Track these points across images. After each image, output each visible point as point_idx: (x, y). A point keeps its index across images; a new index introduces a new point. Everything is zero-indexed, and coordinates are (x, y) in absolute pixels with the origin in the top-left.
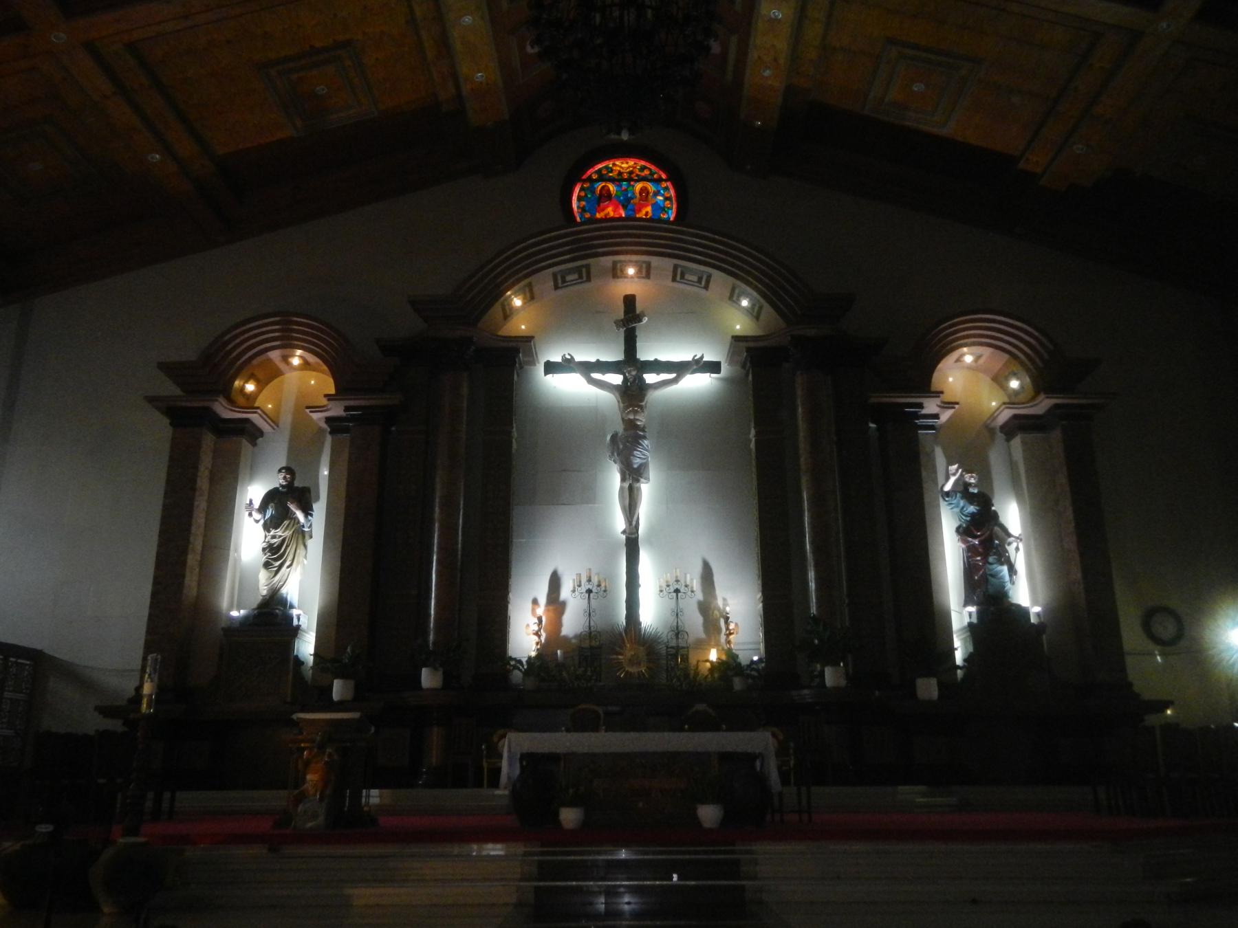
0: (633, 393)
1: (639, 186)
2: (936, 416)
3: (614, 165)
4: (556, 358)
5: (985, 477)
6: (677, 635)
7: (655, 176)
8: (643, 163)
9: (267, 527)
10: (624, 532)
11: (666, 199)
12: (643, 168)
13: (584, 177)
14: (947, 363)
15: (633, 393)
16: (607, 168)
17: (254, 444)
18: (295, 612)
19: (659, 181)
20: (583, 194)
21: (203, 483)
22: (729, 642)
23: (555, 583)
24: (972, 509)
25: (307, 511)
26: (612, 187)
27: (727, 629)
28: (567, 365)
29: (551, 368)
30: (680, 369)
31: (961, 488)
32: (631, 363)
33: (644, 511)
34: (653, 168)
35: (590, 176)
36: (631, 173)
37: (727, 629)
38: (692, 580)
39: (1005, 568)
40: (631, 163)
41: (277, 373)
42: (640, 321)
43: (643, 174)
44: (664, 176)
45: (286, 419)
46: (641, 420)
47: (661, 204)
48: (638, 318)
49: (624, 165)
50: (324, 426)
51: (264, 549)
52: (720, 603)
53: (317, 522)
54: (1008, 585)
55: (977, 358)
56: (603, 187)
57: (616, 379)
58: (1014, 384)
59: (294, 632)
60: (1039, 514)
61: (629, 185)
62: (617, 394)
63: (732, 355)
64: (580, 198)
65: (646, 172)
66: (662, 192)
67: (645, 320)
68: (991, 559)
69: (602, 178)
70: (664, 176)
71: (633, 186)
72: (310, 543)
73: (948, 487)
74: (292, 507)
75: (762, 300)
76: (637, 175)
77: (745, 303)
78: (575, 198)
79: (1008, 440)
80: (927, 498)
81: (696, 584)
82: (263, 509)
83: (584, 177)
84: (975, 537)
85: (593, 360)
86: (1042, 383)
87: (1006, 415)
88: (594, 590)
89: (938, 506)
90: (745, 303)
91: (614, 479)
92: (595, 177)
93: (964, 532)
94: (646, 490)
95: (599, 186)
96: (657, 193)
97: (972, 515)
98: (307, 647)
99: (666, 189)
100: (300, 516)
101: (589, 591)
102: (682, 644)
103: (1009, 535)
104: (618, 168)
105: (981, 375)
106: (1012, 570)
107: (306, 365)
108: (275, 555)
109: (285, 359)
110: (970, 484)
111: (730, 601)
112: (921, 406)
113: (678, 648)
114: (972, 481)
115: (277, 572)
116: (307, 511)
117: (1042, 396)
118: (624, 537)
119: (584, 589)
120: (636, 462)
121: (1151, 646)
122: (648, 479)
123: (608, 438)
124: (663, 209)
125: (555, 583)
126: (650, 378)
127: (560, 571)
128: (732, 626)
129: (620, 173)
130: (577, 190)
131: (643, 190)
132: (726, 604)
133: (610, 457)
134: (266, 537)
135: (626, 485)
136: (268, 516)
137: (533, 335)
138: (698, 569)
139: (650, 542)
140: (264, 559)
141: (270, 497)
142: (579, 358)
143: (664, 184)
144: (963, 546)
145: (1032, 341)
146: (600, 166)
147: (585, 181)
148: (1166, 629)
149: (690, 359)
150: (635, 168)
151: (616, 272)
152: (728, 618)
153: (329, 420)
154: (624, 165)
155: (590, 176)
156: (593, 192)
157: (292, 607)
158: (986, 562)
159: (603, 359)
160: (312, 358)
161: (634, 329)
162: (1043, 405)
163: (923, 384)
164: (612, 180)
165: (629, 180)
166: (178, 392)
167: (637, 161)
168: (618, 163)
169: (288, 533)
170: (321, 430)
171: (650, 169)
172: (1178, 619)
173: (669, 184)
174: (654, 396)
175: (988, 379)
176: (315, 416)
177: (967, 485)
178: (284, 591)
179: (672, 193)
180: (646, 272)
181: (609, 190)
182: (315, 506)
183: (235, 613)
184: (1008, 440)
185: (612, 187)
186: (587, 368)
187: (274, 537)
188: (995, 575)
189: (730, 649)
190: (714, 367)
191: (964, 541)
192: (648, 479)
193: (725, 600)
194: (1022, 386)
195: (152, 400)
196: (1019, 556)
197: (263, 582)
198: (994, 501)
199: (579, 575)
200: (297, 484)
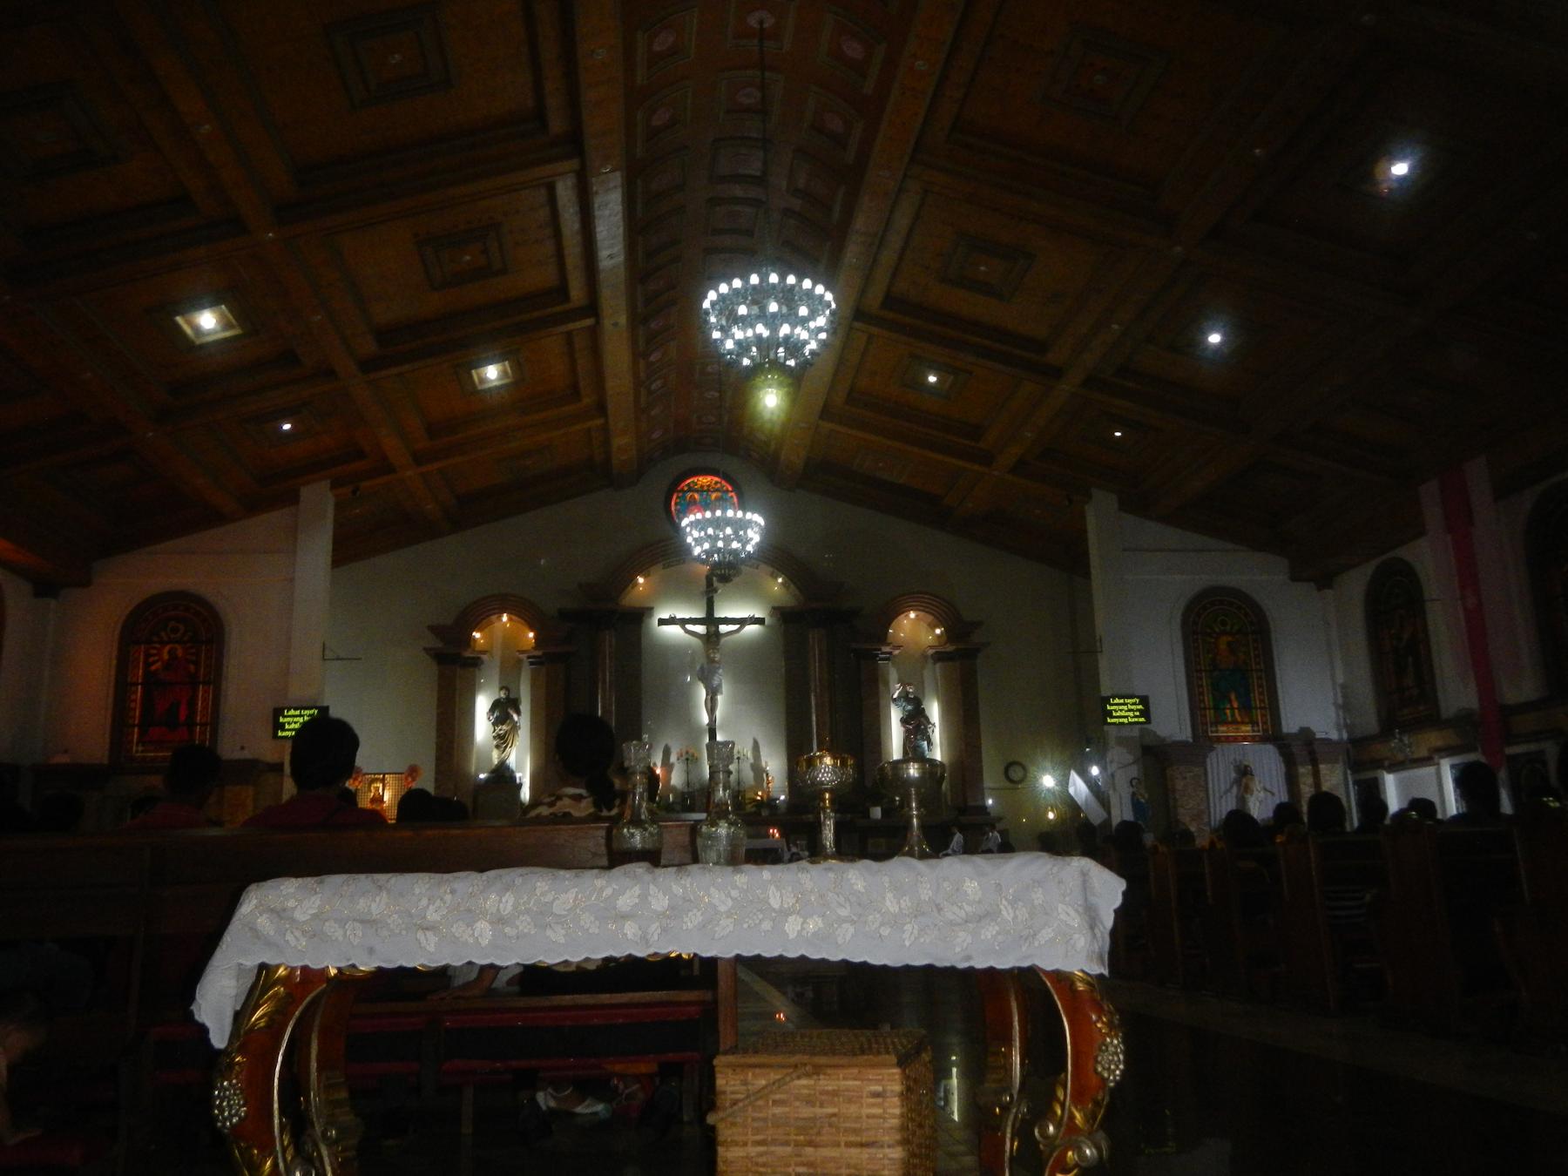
0: (712, 638)
2: (890, 653)
4: (665, 616)
5: (921, 686)
6: (739, 783)
8: (716, 479)
9: (493, 724)
10: (708, 725)
12: (716, 483)
14: (903, 616)
15: (712, 638)
16: (693, 482)
17: (479, 669)
18: (518, 775)
21: (457, 699)
22: (769, 788)
23: (667, 753)
24: (909, 707)
25: (519, 713)
26: (696, 496)
27: (768, 780)
28: (672, 621)
29: (662, 622)
30: (742, 622)
31: (903, 695)
32: (710, 620)
33: (718, 713)
34: (724, 483)
35: (682, 489)
36: (709, 486)
37: (768, 780)
38: (747, 752)
39: (926, 743)
40: (709, 479)
41: (492, 623)
42: (716, 592)
45: (497, 653)
46: (718, 657)
48: (715, 591)
50: (525, 659)
51: (494, 737)
52: (763, 764)
53: (523, 720)
54: (927, 752)
55: (917, 616)
57: (700, 629)
58: (938, 631)
59: (520, 785)
60: (946, 712)
61: (707, 495)
62: (702, 641)
63: (771, 616)
64: (676, 504)
65: (719, 485)
67: (720, 591)
68: (919, 737)
69: (690, 490)
70: (730, 489)
72: (519, 732)
73: (895, 696)
74: (511, 712)
75: (789, 582)
77: (780, 580)
78: (673, 503)
79: (935, 663)
80: (882, 702)
81: (750, 755)
82: (492, 710)
83: (679, 488)
84: (911, 724)
85: (687, 617)
86: (952, 634)
87: (931, 652)
88: (690, 758)
89: (890, 704)
90: (780, 580)
91: (702, 693)
92: (686, 489)
93: (904, 721)
94: (719, 698)
95: (689, 494)
97: (909, 711)
98: (526, 794)
100: (515, 717)
101: (687, 759)
102: (742, 789)
103: (930, 723)
105: (922, 623)
106: (930, 743)
107: (510, 620)
108: (502, 741)
109: (500, 618)
110: (909, 692)
111: (769, 764)
112: (880, 650)
113: (739, 792)
114: (911, 690)
115: (504, 751)
116: (519, 713)
117: (948, 645)
118: (707, 727)
119: (684, 757)
120: (716, 683)
121: (1011, 785)
122: (722, 693)
123: (698, 667)
125: (667, 753)
126: (723, 628)
127: (670, 744)
128: (770, 778)
129: (702, 486)
130: (675, 497)
132: (767, 765)
133: (700, 679)
134: (495, 730)
135: (709, 697)
136: (495, 715)
137: (651, 605)
138: (750, 744)
139: (722, 727)
140: (495, 742)
141: (496, 706)
142: (679, 616)
143: (730, 494)
144: (902, 729)
145: (945, 609)
146: (689, 481)
147: (680, 491)
148: (1016, 773)
149: (747, 616)
152: (767, 774)
153: (529, 657)
154: (704, 480)
155: (682, 489)
157: (513, 772)
158: (915, 738)
159: (693, 617)
160: (514, 617)
161: (712, 597)
162: (950, 648)
163: (882, 638)
164: (697, 491)
165: (709, 490)
166: (440, 645)
167: (713, 477)
168: (700, 479)
169: (509, 727)
170: (520, 661)
172: (1024, 768)
173: (733, 494)
174: (723, 640)
175: (925, 625)
176: (521, 656)
177: (908, 693)
178: (508, 762)
181: (695, 498)
182: (521, 707)
183: (482, 776)
184: (935, 663)
185: (696, 496)
186: (683, 622)
187: (500, 730)
188: (920, 746)
189: (769, 792)
190: (760, 621)
191: (904, 727)
192: (722, 693)
193: (766, 763)
194: (941, 632)
196: (937, 735)
197: (495, 757)
198: (924, 703)
199: (681, 750)
200: (512, 696)
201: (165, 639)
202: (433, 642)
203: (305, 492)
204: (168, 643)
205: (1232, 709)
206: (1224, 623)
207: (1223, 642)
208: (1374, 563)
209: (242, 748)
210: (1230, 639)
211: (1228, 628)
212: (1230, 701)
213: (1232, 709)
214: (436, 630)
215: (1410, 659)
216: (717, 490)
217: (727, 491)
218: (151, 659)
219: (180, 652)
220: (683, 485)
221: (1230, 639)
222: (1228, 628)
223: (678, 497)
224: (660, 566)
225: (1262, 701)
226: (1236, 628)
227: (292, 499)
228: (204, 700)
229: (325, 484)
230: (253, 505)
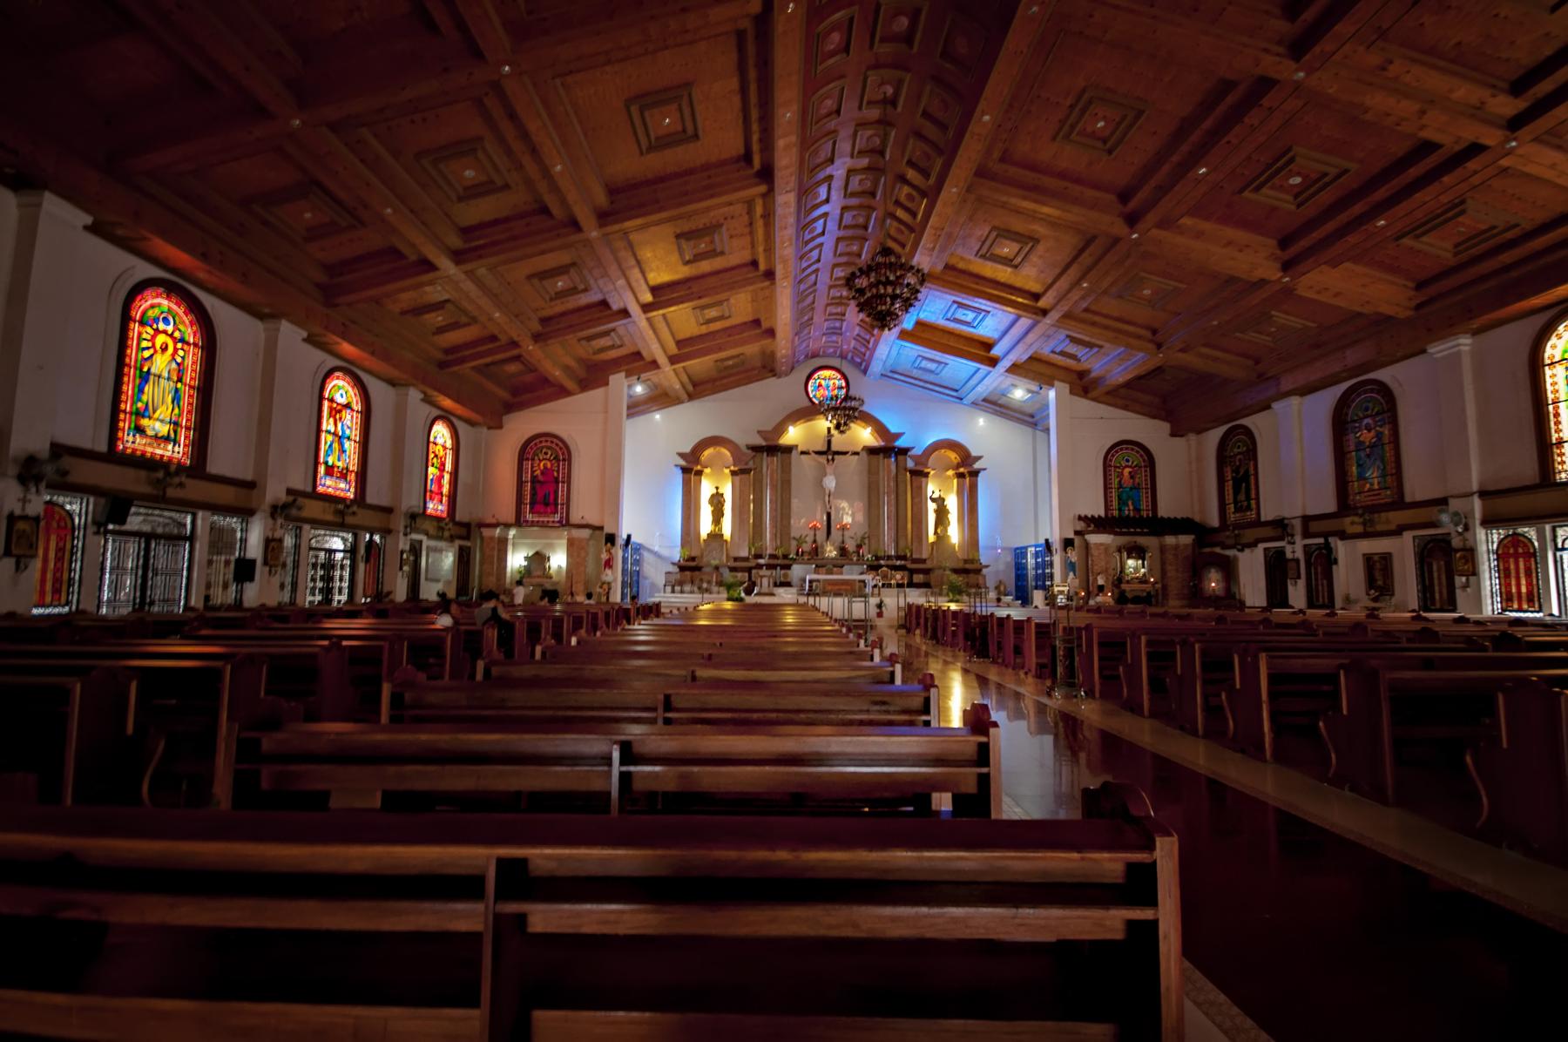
8: (833, 372)
95: (818, 381)
201: (541, 458)
204: (544, 459)
205: (1129, 510)
206: (1127, 460)
207: (1127, 471)
208: (1224, 428)
209: (582, 518)
210: (1130, 470)
211: (1130, 463)
212: (1128, 506)
213: (1129, 510)
214: (682, 455)
215: (1244, 485)
218: (535, 469)
219: (549, 465)
221: (1130, 470)
222: (1130, 463)
224: (802, 421)
225: (1147, 506)
226: (1135, 463)
228: (563, 491)
229: (623, 374)
230: (585, 385)
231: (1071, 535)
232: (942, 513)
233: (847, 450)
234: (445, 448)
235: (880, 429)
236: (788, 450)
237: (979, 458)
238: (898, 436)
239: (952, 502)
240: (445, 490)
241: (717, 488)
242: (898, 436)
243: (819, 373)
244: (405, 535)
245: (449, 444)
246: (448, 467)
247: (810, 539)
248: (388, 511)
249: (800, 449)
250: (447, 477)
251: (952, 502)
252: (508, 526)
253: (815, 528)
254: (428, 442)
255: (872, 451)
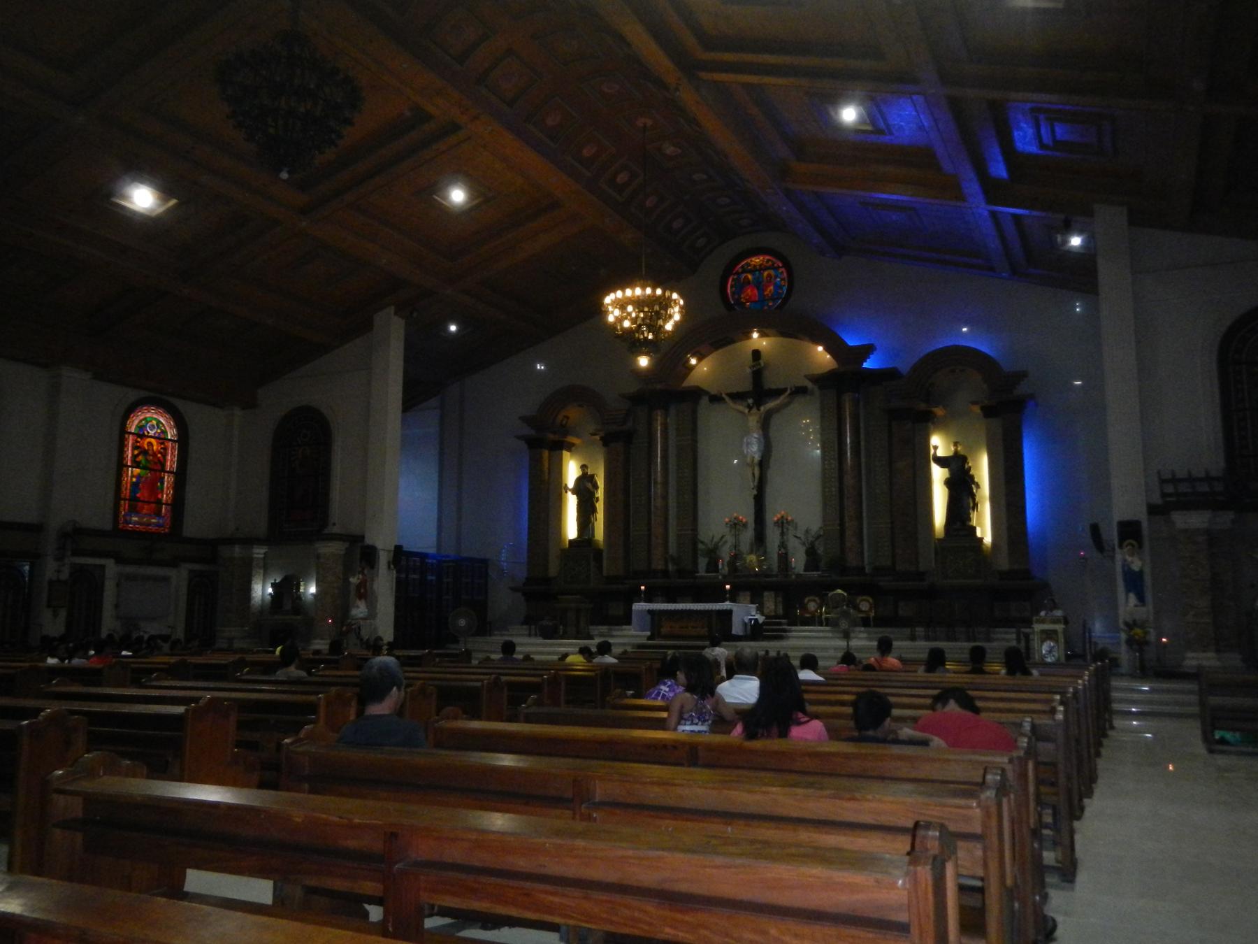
1: (766, 273)
3: (751, 261)
7: (776, 265)
8: (767, 257)
11: (782, 279)
12: (768, 260)
13: (734, 272)
19: (776, 269)
20: (733, 283)
26: (750, 277)
34: (774, 260)
36: (760, 265)
40: (761, 258)
43: (768, 265)
44: (781, 265)
47: (778, 283)
49: (758, 260)
56: (745, 277)
64: (732, 287)
65: (770, 263)
66: (779, 275)
69: (744, 271)
70: (781, 265)
71: (762, 274)
76: (765, 266)
83: (734, 272)
92: (740, 270)
93: (948, 483)
95: (743, 276)
96: (776, 277)
99: (782, 273)
104: (753, 263)
124: (781, 287)
129: (755, 266)
130: (731, 280)
131: (769, 275)
147: (734, 274)
150: (763, 261)
151: (748, 336)
154: (757, 260)
156: (738, 279)
164: (751, 272)
168: (753, 259)
171: (772, 261)
173: (783, 269)
179: (785, 274)
180: (762, 335)
181: (748, 279)
185: (750, 277)
195: (519, 437)
202: (528, 431)
203: (379, 319)
214: (526, 420)
216: (766, 268)
217: (779, 267)
220: (736, 269)
223: (733, 280)
227: (366, 326)
229: (392, 310)
231: (1141, 514)
232: (961, 486)
233: (782, 386)
234: (161, 439)
235: (835, 347)
236: (696, 394)
237: (1021, 376)
238: (866, 351)
239: (982, 469)
240: (166, 495)
241: (583, 467)
242: (866, 351)
243: (749, 260)
244: (60, 558)
245: (171, 433)
246: (171, 462)
247: (730, 540)
248: (36, 529)
249: (713, 392)
250: (168, 480)
251: (982, 469)
252: (249, 541)
253: (736, 525)
254: (123, 432)
255: (825, 381)
